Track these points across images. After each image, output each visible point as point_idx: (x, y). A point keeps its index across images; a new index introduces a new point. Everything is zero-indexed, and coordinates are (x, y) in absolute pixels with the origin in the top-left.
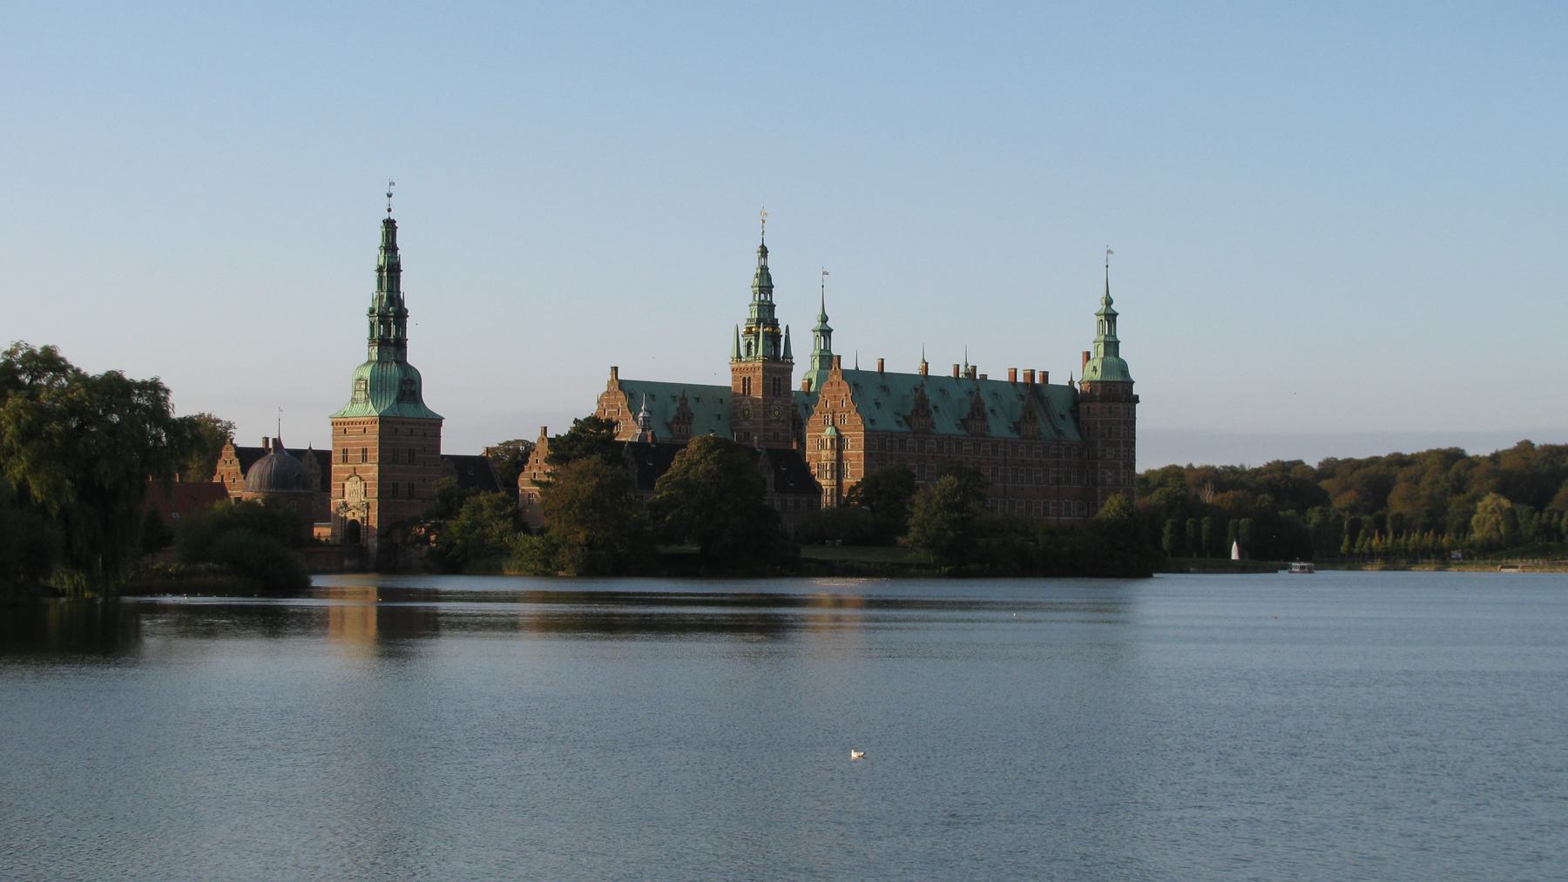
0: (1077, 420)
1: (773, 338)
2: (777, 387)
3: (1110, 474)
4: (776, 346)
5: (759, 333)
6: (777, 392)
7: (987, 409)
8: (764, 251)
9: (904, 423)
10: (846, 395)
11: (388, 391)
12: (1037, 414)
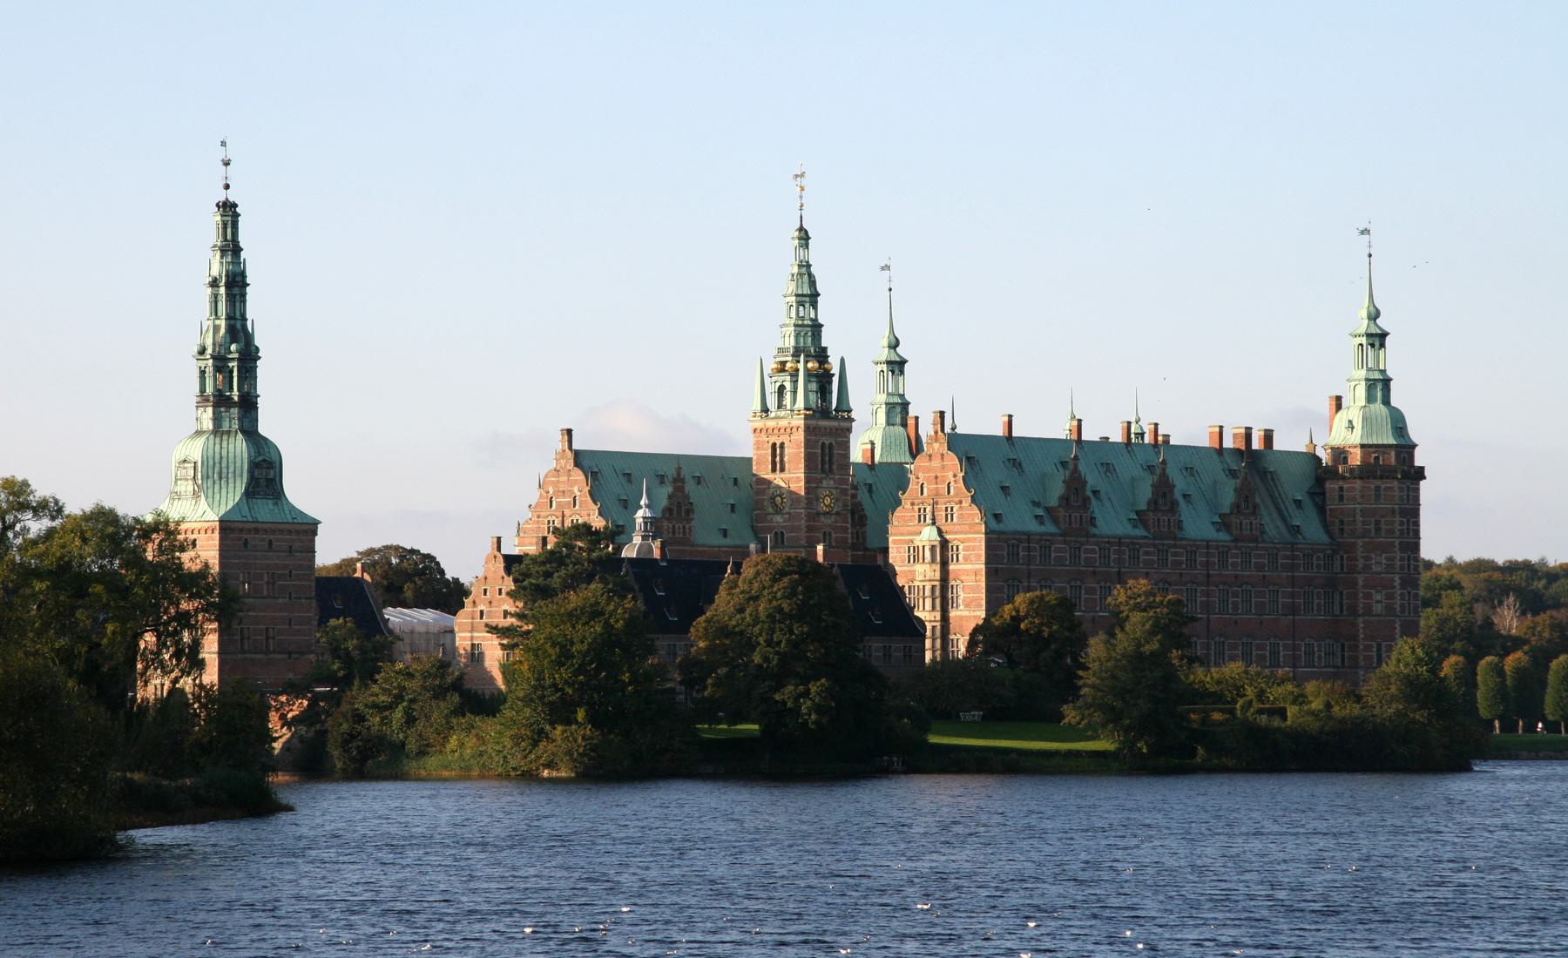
0: (1321, 510)
1: (822, 379)
4: (824, 391)
5: (797, 370)
6: (827, 466)
7: (1178, 495)
8: (804, 237)
10: (955, 476)
11: (231, 481)
12: (1258, 500)
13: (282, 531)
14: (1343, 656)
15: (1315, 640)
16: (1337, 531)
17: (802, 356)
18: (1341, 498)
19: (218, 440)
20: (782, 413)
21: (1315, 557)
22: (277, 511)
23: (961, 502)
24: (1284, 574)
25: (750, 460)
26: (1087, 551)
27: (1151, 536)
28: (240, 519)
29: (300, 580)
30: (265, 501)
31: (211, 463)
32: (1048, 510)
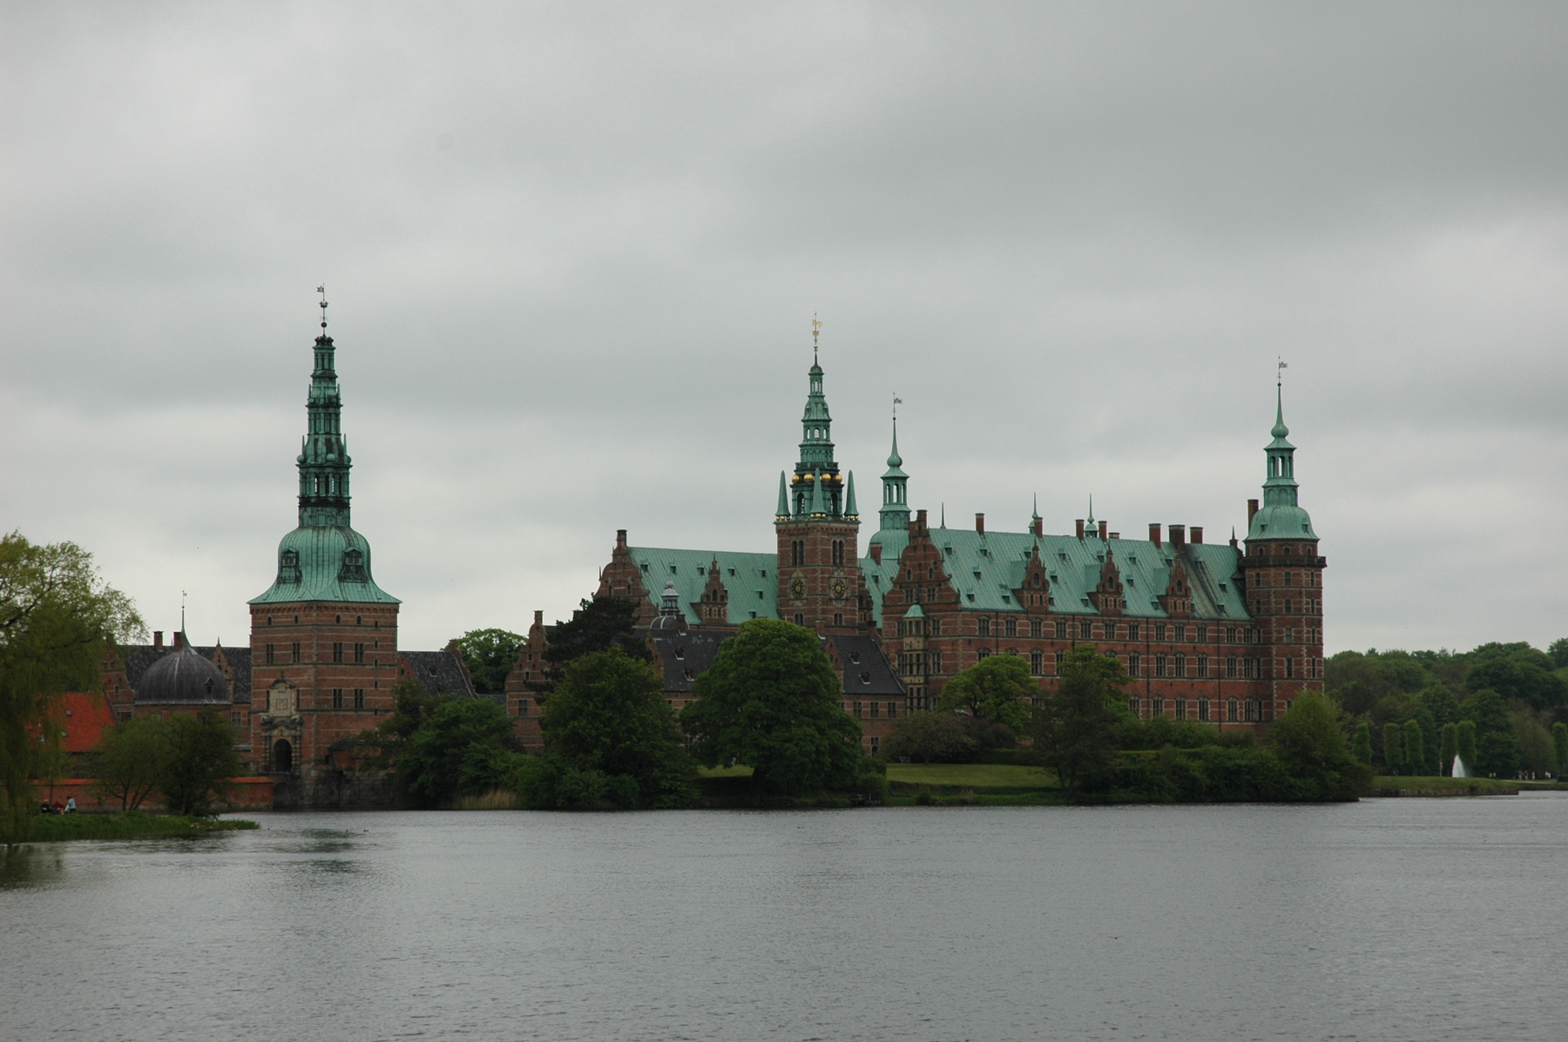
0: (1242, 592)
4: (836, 498)
6: (838, 560)
7: (1122, 579)
8: (816, 374)
9: (1012, 599)
11: (326, 567)
12: (1189, 584)
13: (368, 609)
14: (1260, 712)
15: (1237, 699)
16: (1255, 610)
17: (817, 469)
18: (1258, 582)
19: (315, 533)
20: (801, 518)
21: (1237, 631)
22: (365, 593)
23: (940, 585)
24: (1211, 645)
26: (1046, 625)
27: (1100, 614)
28: (333, 599)
29: (385, 650)
30: (354, 584)
31: (310, 552)
32: (1014, 591)
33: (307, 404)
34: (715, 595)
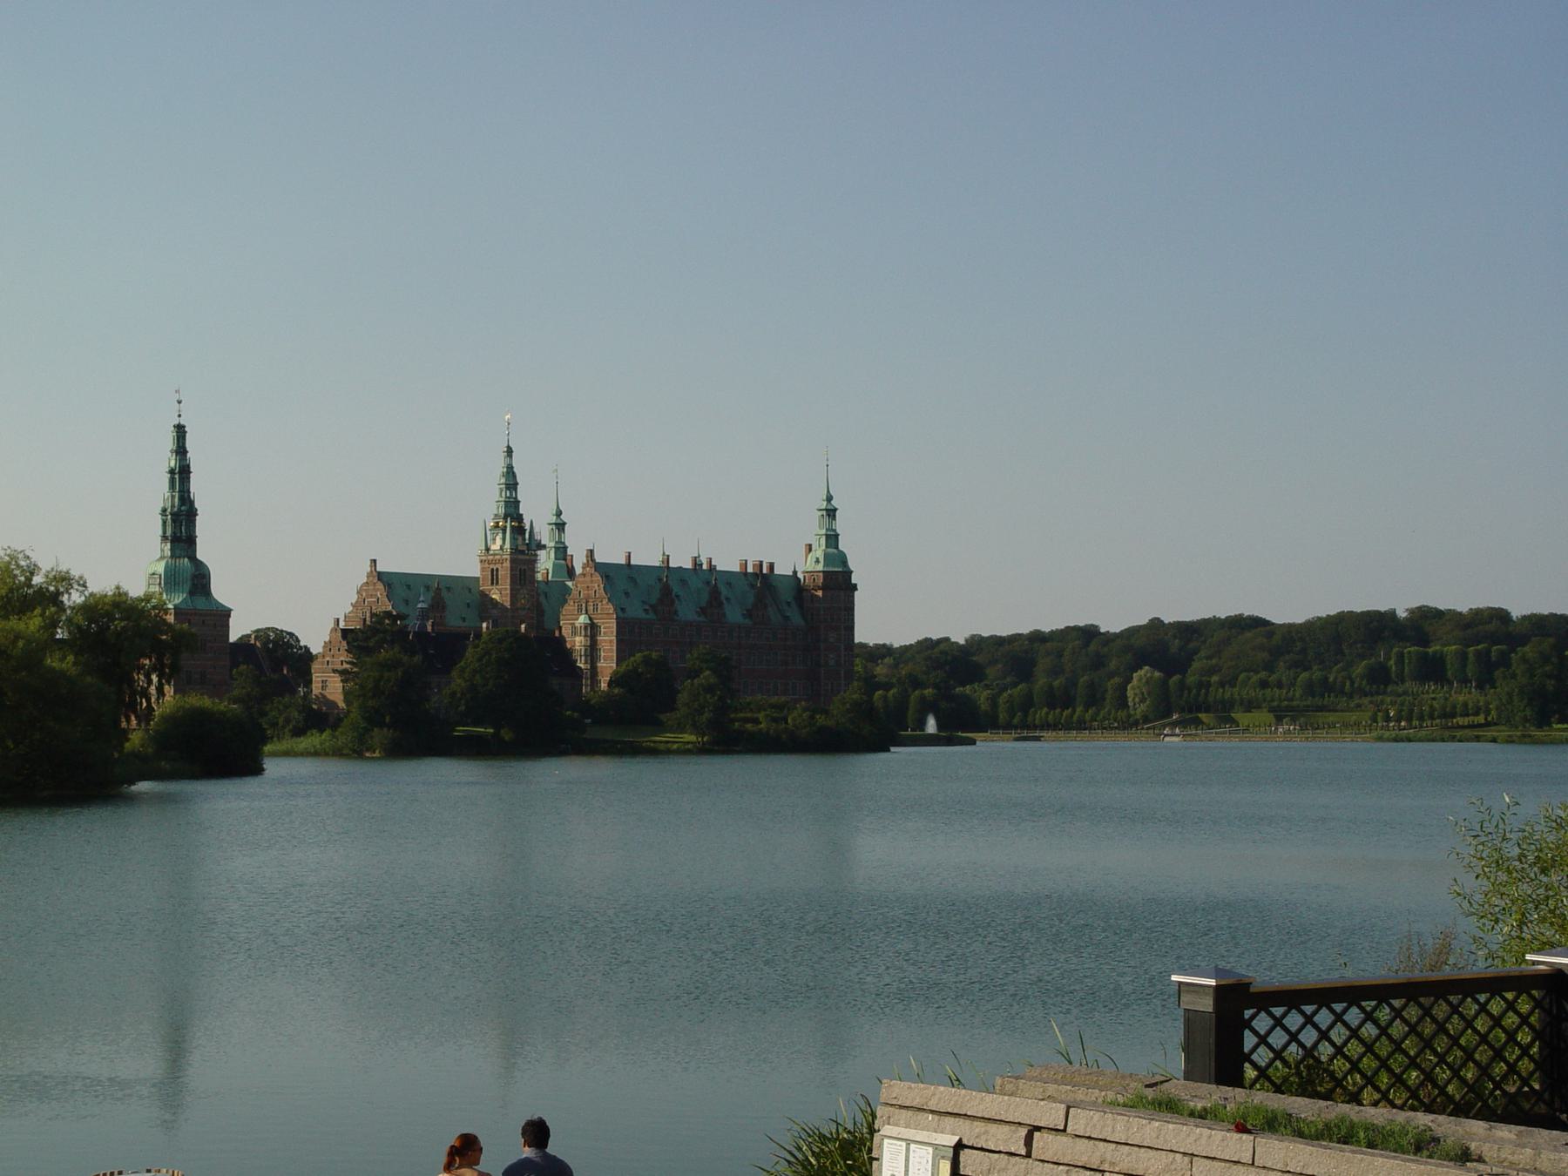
0: (801, 607)
1: (519, 530)
2: (522, 577)
3: (831, 656)
5: (506, 527)
6: (523, 582)
7: (723, 598)
8: (509, 451)
10: (599, 586)
25: (478, 578)
32: (651, 606)
33: (167, 470)
34: (438, 605)
